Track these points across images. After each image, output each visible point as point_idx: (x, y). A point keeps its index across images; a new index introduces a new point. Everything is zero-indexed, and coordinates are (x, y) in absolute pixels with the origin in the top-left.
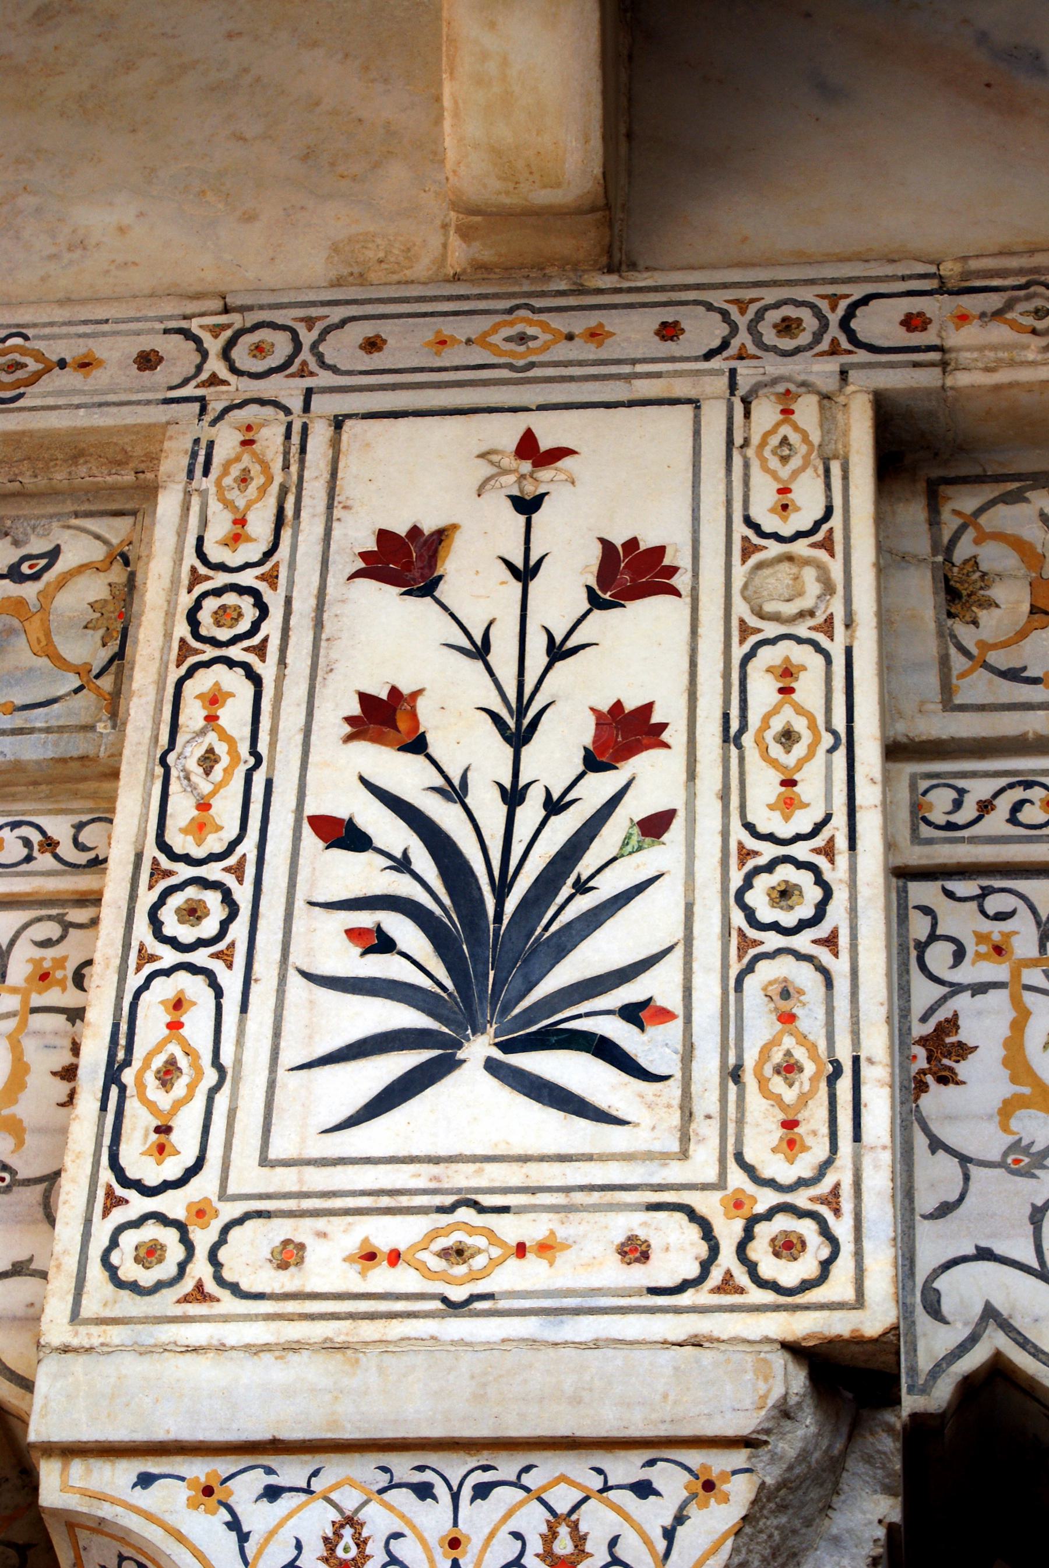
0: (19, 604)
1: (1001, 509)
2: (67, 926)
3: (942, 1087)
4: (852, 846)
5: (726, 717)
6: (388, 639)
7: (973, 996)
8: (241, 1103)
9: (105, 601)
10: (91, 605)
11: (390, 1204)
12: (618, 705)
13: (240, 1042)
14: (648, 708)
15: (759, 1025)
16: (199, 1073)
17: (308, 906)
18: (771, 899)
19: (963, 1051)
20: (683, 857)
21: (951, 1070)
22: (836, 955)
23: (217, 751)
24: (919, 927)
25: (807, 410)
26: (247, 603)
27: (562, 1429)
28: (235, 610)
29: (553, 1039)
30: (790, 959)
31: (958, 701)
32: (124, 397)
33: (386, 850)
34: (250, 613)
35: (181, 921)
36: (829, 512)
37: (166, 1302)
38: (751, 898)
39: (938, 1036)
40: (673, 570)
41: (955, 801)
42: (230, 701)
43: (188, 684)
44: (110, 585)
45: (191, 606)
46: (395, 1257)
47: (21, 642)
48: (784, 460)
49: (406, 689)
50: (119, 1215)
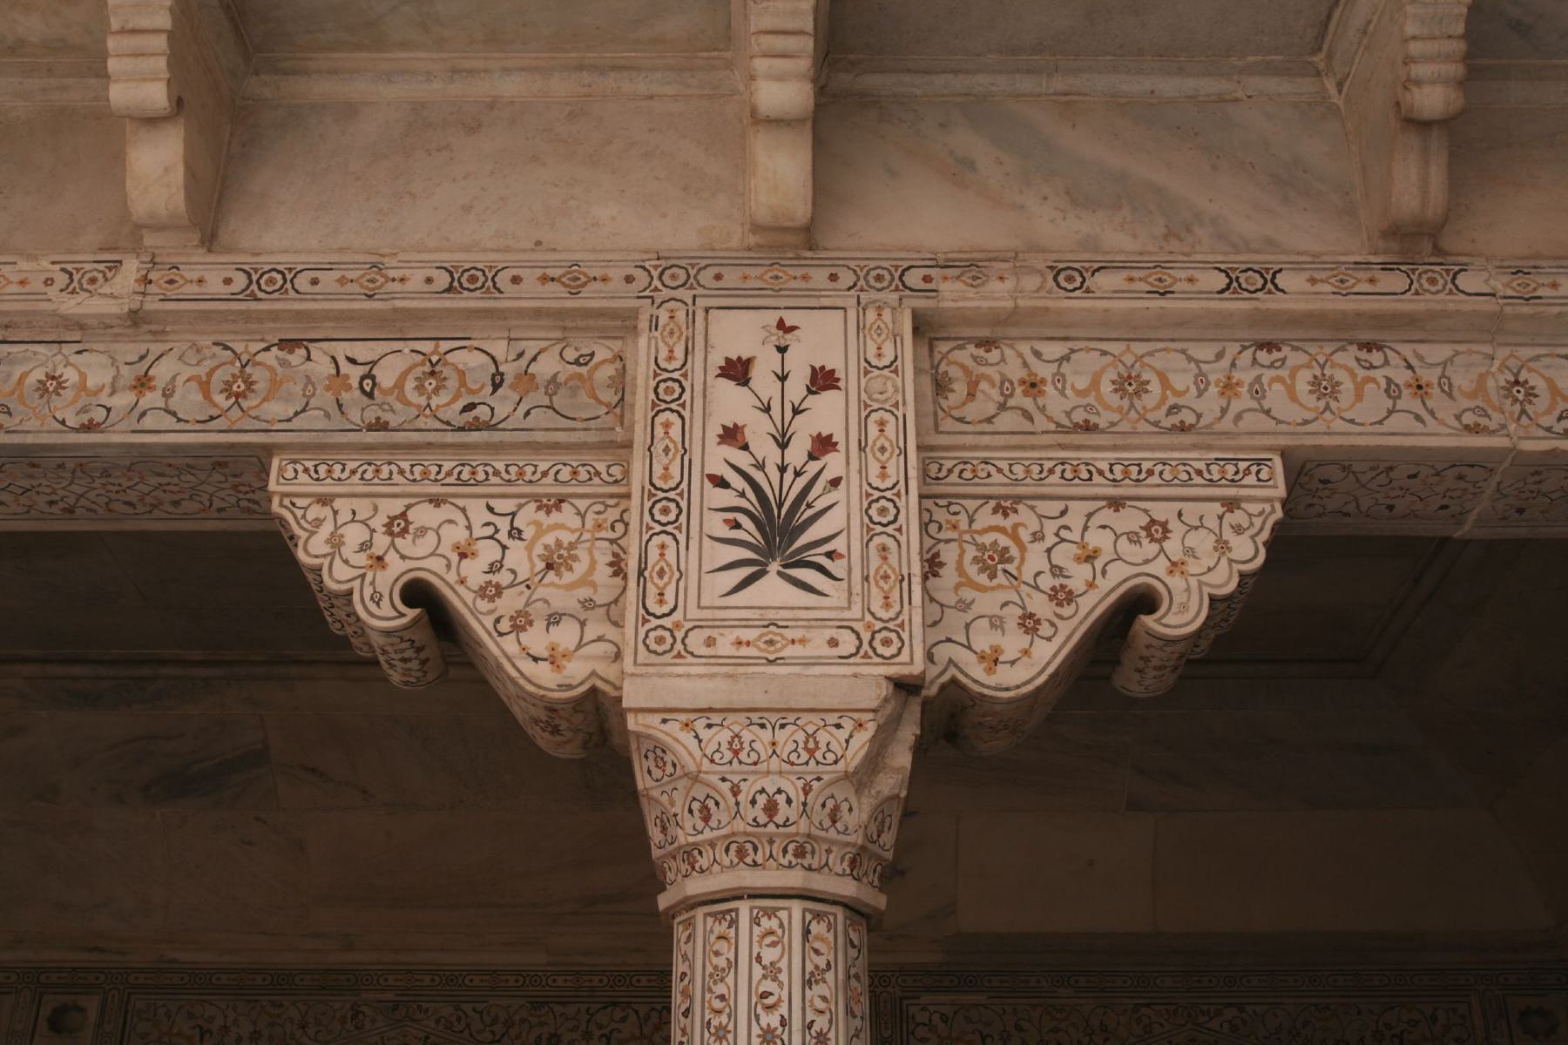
0: (581, 375)
2: (607, 506)
6: (732, 403)
11: (745, 624)
14: (831, 436)
15: (875, 562)
19: (941, 565)
24: (926, 517)
25: (887, 314)
26: (676, 386)
27: (810, 706)
34: (678, 390)
37: (667, 658)
46: (748, 644)
49: (740, 424)
50: (648, 626)
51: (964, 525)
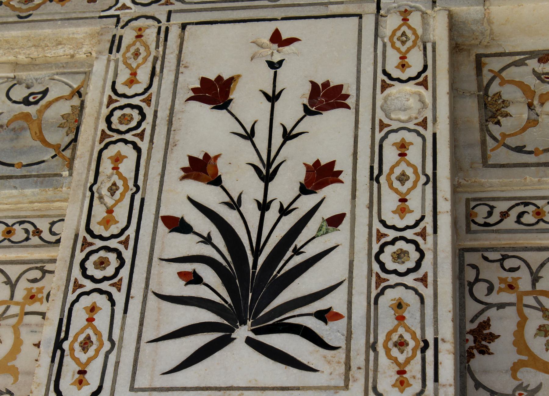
0: (26, 117)
1: (513, 69)
3: (481, 356)
4: (435, 231)
5: (372, 168)
6: (205, 130)
7: (497, 310)
8: (122, 359)
9: (69, 114)
10: (63, 116)
12: (318, 162)
13: (122, 329)
14: (333, 163)
16: (102, 344)
17: (159, 260)
18: (393, 258)
19: (493, 337)
20: (348, 237)
21: (486, 347)
22: (426, 286)
23: (118, 184)
24: (470, 275)
26: (135, 113)
28: (129, 116)
29: (281, 328)
30: (403, 288)
31: (490, 162)
32: (80, 16)
33: (200, 233)
34: (137, 117)
35: (96, 268)
36: (425, 68)
38: (382, 257)
39: (479, 330)
40: (347, 96)
41: (488, 212)
42: (125, 160)
43: (105, 152)
44: (72, 106)
45: (108, 114)
47: (28, 134)
48: (403, 43)
49: (212, 155)
51: (525, 284)
